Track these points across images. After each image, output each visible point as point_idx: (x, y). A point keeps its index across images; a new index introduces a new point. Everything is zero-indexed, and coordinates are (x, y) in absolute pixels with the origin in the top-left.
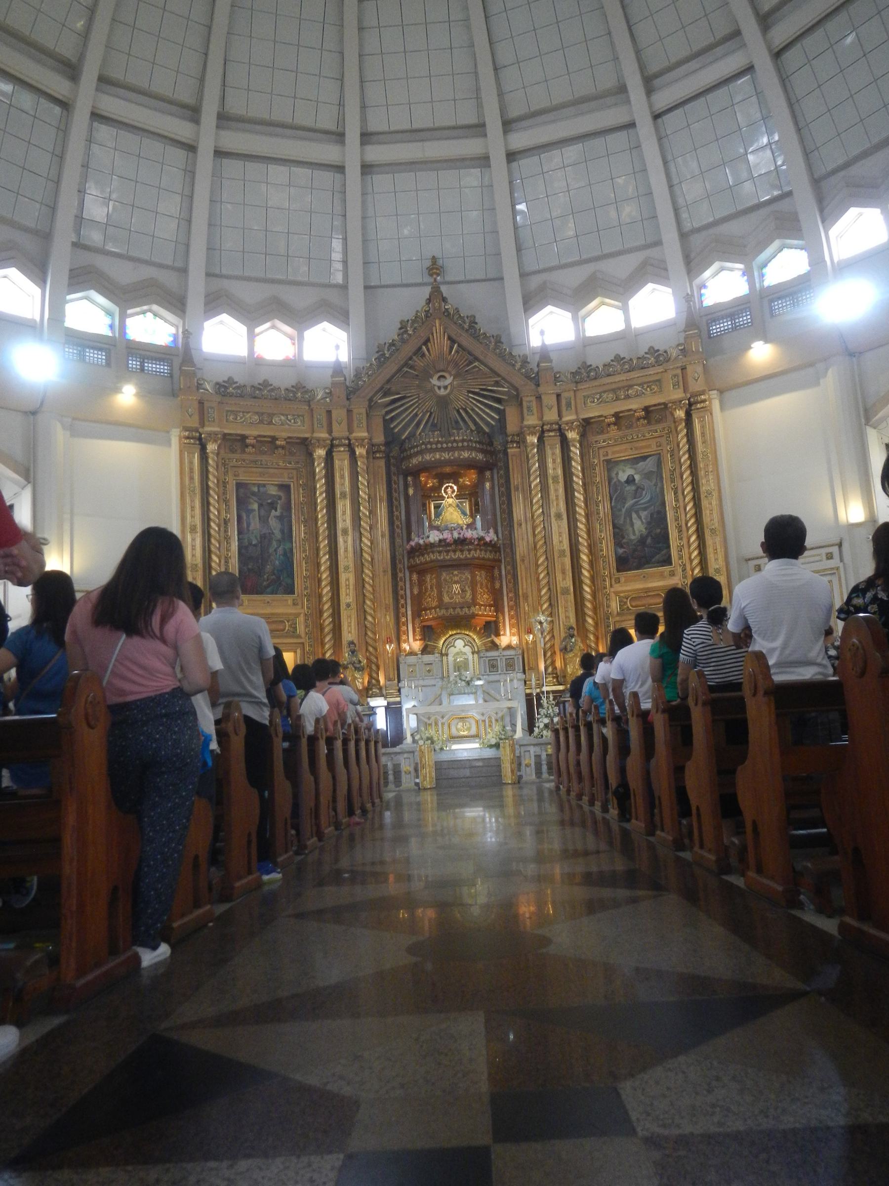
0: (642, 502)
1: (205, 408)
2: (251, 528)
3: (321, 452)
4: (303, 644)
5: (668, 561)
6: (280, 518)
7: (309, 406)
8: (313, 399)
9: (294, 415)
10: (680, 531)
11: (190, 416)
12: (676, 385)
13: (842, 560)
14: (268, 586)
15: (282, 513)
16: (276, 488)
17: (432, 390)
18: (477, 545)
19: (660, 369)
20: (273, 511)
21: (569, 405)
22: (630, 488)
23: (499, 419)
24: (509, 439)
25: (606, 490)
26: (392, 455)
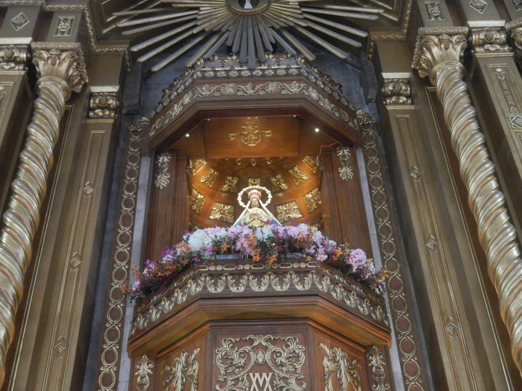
18: (325, 263)
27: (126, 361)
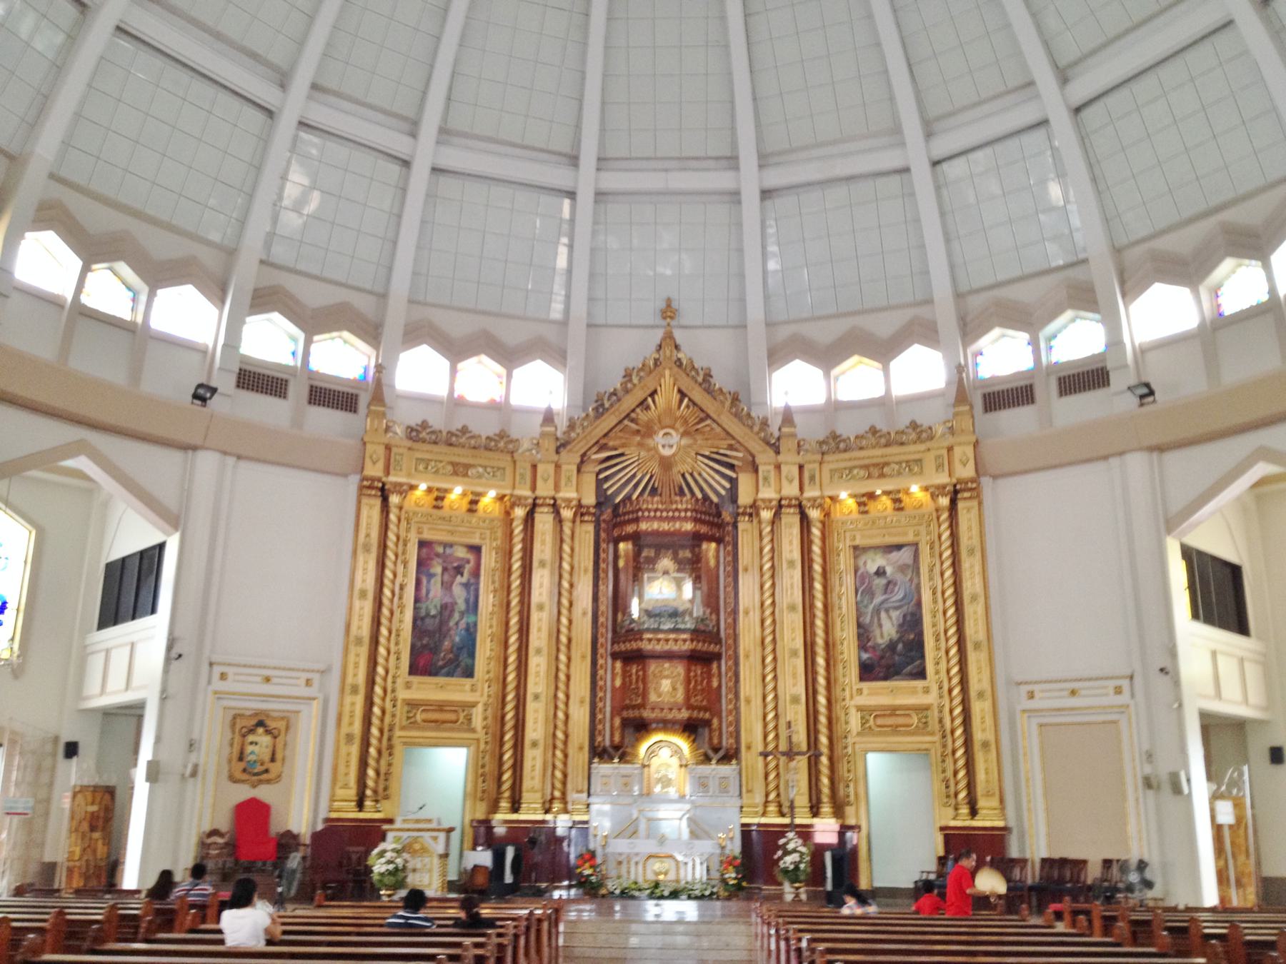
0: (894, 599)
1: (392, 455)
2: (431, 595)
3: (520, 512)
4: (478, 740)
5: (921, 674)
6: (466, 586)
7: (513, 457)
8: (517, 450)
9: (493, 468)
10: (937, 640)
11: (374, 463)
12: (939, 467)
13: (1133, 695)
14: (442, 667)
15: (469, 580)
16: (465, 550)
17: (655, 449)
19: (922, 447)
20: (459, 577)
21: (812, 478)
22: (881, 582)
23: (731, 488)
24: (741, 510)
25: (849, 580)
26: (602, 518)
27: (610, 661)
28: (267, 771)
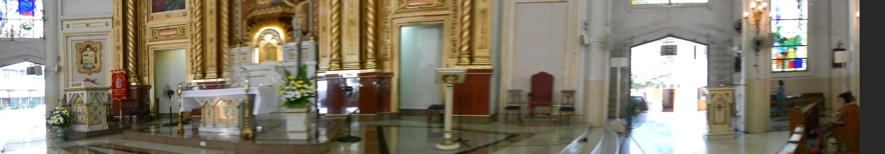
28: (94, 67)
